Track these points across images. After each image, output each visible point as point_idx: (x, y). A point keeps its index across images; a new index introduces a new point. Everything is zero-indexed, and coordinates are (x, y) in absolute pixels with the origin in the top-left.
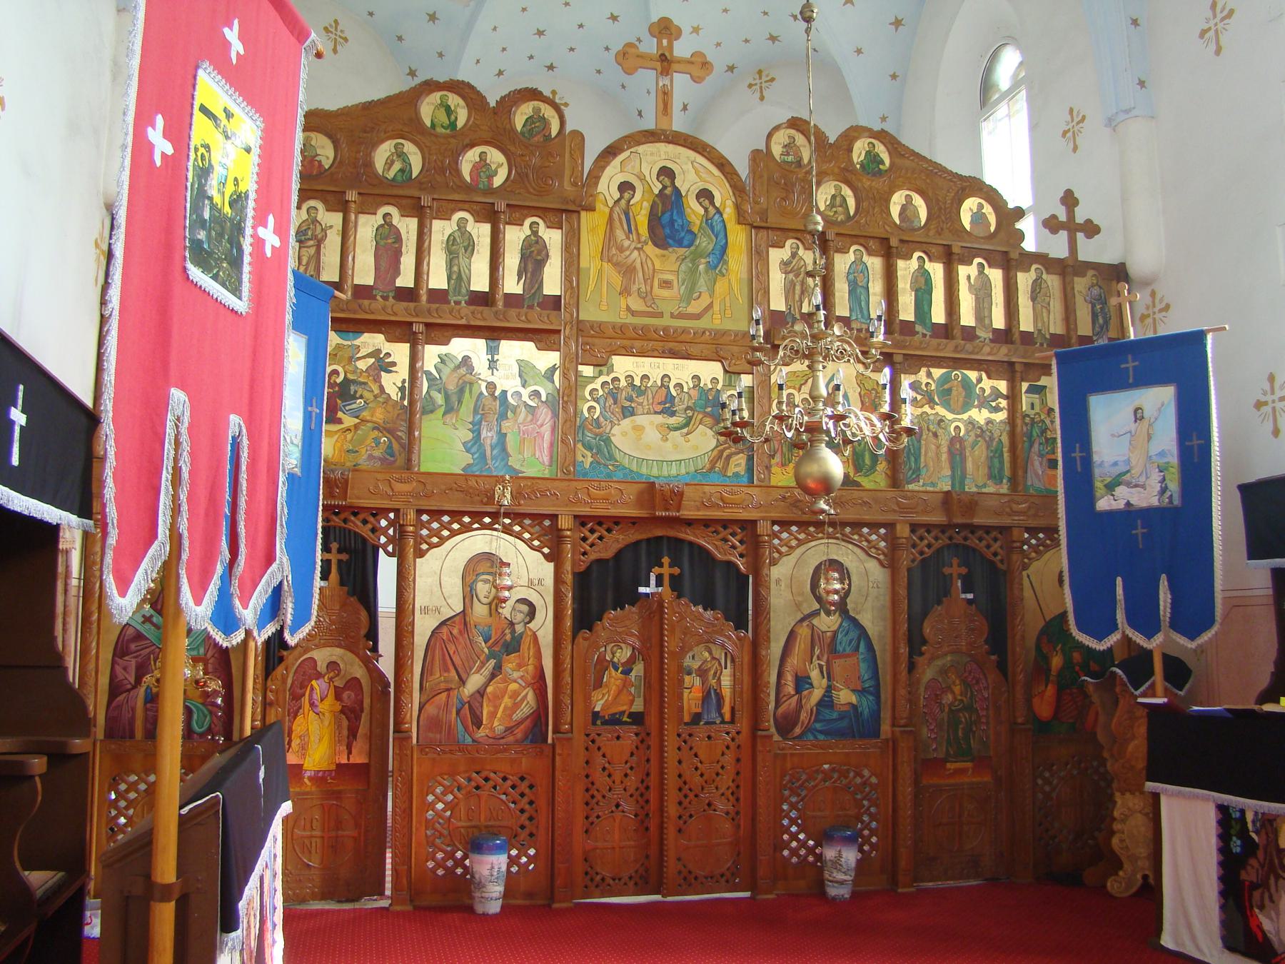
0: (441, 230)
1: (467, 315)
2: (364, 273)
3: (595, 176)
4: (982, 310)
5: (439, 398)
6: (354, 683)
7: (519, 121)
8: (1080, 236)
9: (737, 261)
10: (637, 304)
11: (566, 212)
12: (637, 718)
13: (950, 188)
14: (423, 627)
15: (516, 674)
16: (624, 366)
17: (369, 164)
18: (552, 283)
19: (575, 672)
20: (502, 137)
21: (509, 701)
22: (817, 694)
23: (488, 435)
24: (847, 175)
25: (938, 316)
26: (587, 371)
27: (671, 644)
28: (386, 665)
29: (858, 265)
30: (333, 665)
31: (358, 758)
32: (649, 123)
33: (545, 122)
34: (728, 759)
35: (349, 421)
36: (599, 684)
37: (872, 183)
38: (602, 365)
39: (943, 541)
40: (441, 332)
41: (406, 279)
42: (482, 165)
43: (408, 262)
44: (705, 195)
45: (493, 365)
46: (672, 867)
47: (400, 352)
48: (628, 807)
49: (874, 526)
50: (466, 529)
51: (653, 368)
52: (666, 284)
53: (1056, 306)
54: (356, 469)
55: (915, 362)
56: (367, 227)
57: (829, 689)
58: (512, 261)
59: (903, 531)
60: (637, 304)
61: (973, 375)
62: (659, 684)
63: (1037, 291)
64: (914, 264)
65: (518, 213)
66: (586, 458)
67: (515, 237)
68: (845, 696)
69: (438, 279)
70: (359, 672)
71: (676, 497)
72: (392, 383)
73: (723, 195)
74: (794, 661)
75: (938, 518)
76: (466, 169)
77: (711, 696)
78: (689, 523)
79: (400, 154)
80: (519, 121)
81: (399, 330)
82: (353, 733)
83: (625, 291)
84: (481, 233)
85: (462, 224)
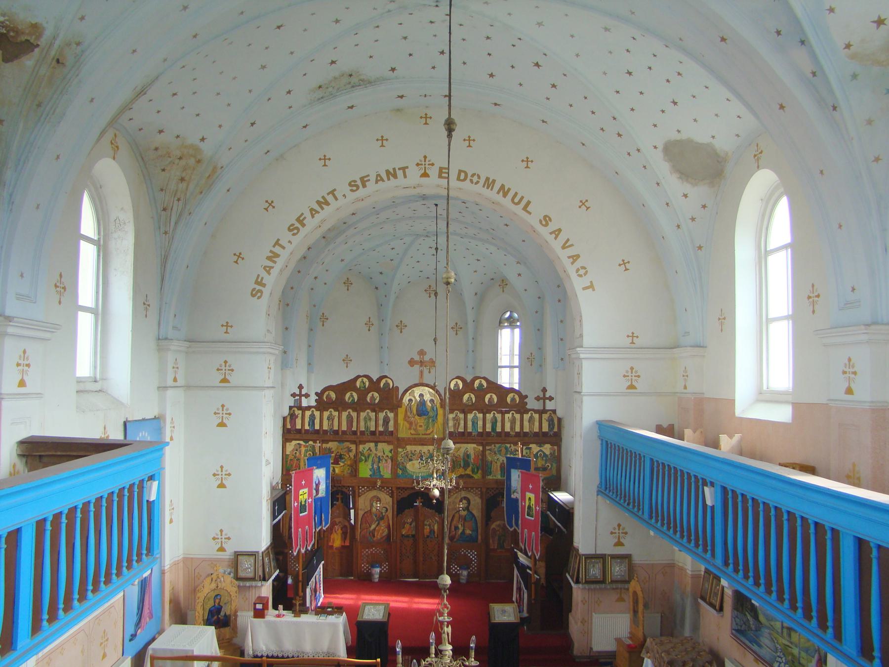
0: (363, 415)
2: (344, 427)
3: (402, 398)
4: (512, 428)
6: (345, 527)
7: (382, 385)
8: (547, 401)
9: (440, 419)
12: (413, 536)
13: (503, 392)
14: (361, 513)
15: (383, 525)
16: (409, 448)
18: (391, 428)
20: (378, 390)
21: (381, 531)
22: (461, 531)
23: (375, 466)
24: (472, 390)
25: (499, 429)
26: (400, 450)
28: (352, 522)
29: (475, 417)
31: (347, 543)
32: (417, 382)
33: (389, 384)
35: (342, 464)
37: (480, 393)
38: (403, 448)
40: (364, 442)
41: (354, 429)
43: (355, 424)
44: (432, 401)
47: (353, 447)
49: (477, 488)
51: (418, 448)
52: (421, 426)
53: (537, 424)
55: (489, 444)
56: (345, 415)
58: (381, 422)
59: (484, 490)
60: (413, 432)
61: (508, 445)
62: (419, 527)
63: (531, 420)
64: (492, 415)
65: (382, 410)
66: (400, 472)
67: (381, 415)
68: (468, 532)
70: (347, 524)
72: (352, 454)
73: (437, 400)
74: (454, 522)
76: (368, 399)
77: (432, 531)
79: (352, 396)
80: (382, 385)
83: (410, 429)
84: (373, 415)
85: (368, 414)
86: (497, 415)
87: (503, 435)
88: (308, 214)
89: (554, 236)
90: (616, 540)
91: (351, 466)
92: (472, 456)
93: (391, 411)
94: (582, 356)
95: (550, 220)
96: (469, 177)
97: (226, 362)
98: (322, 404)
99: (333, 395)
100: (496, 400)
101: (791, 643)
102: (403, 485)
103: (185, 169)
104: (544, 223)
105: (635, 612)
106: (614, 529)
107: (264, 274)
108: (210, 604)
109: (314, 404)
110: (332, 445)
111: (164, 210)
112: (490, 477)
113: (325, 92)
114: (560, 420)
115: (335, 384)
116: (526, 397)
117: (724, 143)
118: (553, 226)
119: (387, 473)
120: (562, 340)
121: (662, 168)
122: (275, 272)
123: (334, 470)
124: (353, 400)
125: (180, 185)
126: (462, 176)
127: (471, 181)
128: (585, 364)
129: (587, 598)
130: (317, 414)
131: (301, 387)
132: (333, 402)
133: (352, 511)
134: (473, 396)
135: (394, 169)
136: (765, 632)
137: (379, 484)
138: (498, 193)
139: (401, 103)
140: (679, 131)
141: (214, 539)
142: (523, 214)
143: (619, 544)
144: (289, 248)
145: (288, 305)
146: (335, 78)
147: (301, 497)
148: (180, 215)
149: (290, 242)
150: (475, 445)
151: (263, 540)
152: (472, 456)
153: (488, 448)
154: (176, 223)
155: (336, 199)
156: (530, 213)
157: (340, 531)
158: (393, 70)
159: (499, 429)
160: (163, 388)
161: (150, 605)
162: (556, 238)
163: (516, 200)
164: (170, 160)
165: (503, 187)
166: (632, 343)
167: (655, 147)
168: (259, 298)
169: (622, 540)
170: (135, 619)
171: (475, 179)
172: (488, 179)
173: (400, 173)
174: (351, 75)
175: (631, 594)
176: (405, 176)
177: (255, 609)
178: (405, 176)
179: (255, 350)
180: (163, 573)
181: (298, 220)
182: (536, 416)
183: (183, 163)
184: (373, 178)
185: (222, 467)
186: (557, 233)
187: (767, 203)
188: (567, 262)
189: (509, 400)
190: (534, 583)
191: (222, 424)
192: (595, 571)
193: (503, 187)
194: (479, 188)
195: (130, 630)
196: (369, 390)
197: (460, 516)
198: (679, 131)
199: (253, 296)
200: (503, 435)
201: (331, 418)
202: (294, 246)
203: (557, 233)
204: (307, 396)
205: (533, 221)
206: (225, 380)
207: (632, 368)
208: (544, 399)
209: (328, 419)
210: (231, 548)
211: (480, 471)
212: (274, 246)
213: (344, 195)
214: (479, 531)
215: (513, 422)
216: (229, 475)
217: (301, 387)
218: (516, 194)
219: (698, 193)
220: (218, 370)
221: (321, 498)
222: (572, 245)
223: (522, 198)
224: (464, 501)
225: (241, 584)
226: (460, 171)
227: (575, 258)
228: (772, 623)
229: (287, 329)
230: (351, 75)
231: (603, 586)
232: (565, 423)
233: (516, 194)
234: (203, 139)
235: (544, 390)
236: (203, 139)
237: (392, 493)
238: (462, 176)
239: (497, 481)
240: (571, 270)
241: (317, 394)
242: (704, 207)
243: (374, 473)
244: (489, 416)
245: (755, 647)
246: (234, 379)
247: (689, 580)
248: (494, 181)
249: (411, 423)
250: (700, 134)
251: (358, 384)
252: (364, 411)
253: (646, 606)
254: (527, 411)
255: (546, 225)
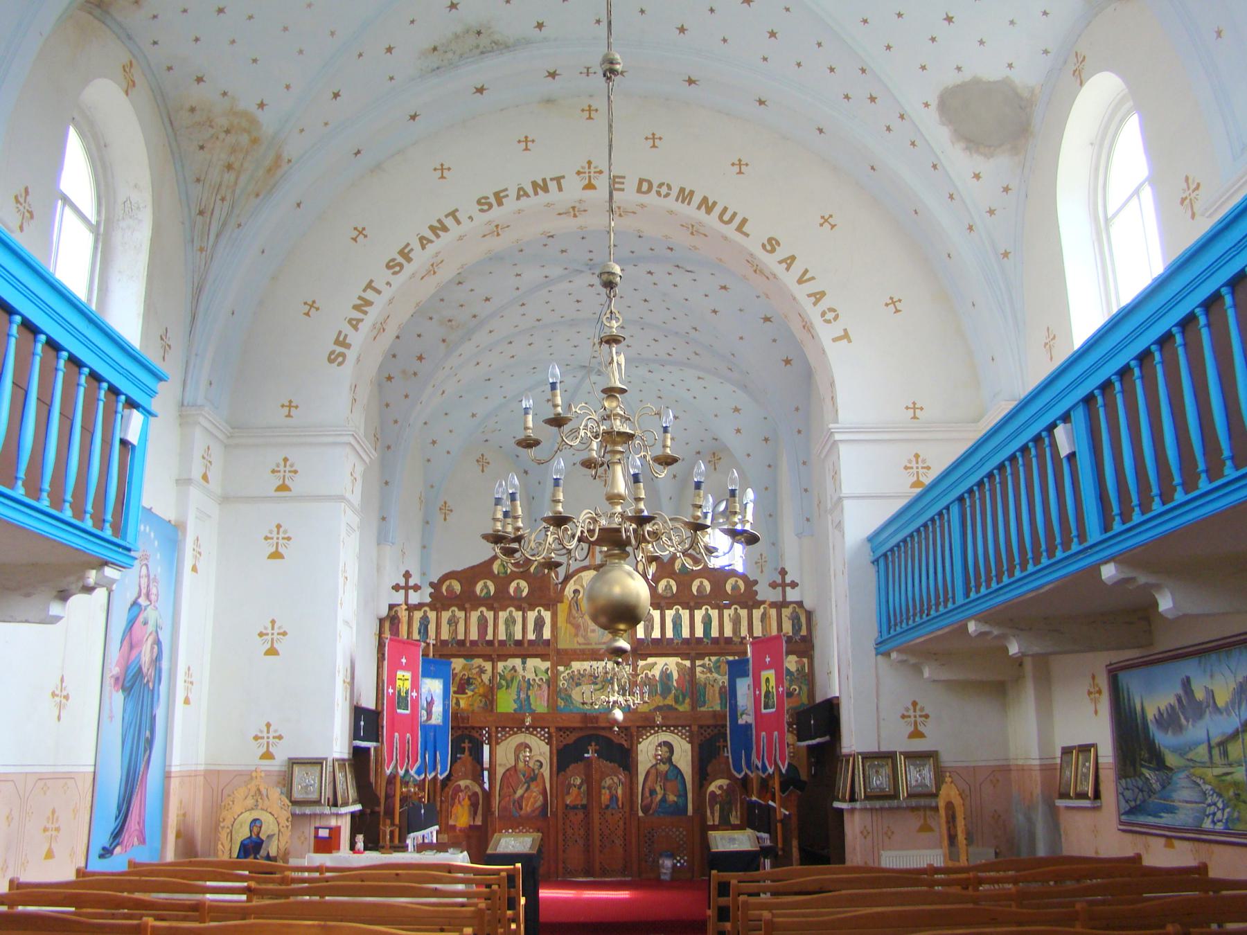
0: (503, 615)
1: (512, 649)
2: (474, 636)
3: (563, 589)
4: (736, 630)
5: (504, 683)
6: (476, 794)
8: (788, 589)
10: (581, 640)
11: (551, 605)
12: (584, 807)
13: (719, 577)
14: (500, 771)
15: (535, 790)
16: (576, 666)
17: (474, 592)
18: (547, 634)
19: (561, 787)
21: (532, 801)
22: (659, 797)
25: (715, 633)
26: (561, 668)
27: (596, 776)
28: (486, 786)
30: (467, 787)
31: (479, 822)
34: (621, 823)
35: (470, 693)
36: (568, 793)
38: (567, 665)
39: (716, 731)
40: (503, 657)
41: (489, 637)
42: (518, 588)
45: (524, 669)
46: (597, 866)
47: (488, 666)
48: (581, 842)
49: (684, 727)
50: (515, 733)
54: (473, 712)
55: (701, 656)
56: (474, 616)
57: (664, 795)
59: (695, 728)
60: (581, 640)
63: (764, 617)
64: (703, 611)
66: (561, 703)
67: (532, 616)
68: (672, 798)
69: (502, 636)
70: (477, 789)
71: (596, 718)
74: (649, 783)
75: (711, 722)
76: (511, 591)
77: (613, 798)
78: (603, 728)
79: (486, 586)
81: (487, 658)
82: (475, 813)
83: (576, 635)
84: (518, 615)
85: (511, 613)
86: (710, 611)
87: (722, 642)
88: (415, 244)
89: (784, 265)
90: (912, 729)
91: (485, 696)
92: (675, 676)
93: (547, 608)
94: (837, 437)
95: (778, 243)
96: (655, 188)
97: (286, 460)
98: (440, 601)
99: (457, 587)
100: (708, 589)
101: (1230, 765)
102: (566, 724)
103: (233, 151)
104: (769, 248)
105: (952, 839)
106: (907, 709)
107: (347, 329)
108: (243, 833)
109: (428, 600)
110: (458, 664)
111: (201, 213)
112: (703, 709)
113: (441, 57)
114: (809, 614)
115: (459, 569)
116: (756, 582)
117: (1026, 76)
118: (781, 253)
119: (540, 706)
120: (806, 490)
121: (939, 135)
122: (365, 327)
123: (458, 703)
124: (489, 592)
125: (226, 176)
126: (645, 186)
127: (659, 193)
128: (843, 448)
129: (870, 829)
130: (432, 615)
131: (407, 575)
132: (457, 597)
133: (486, 773)
134: (673, 583)
135: (544, 180)
136: (1180, 779)
137: (528, 721)
138: (699, 208)
139: (554, 86)
140: (959, 69)
141: (256, 738)
142: (738, 237)
143: (916, 734)
144: (387, 293)
145: (389, 447)
146: (457, 36)
147: (399, 683)
148: (224, 224)
149: (388, 284)
150: (678, 659)
151: (338, 745)
152: (675, 676)
153: (698, 663)
154: (218, 235)
155: (458, 222)
156: (747, 235)
157: (466, 802)
158: (540, 26)
159: (715, 633)
160: (183, 482)
161: (141, 822)
162: (788, 269)
163: (726, 218)
164: (212, 131)
165: (705, 200)
166: (915, 417)
167: (926, 105)
168: (340, 364)
169: (921, 728)
170: (112, 825)
171: (664, 190)
172: (682, 190)
173: (552, 186)
174: (479, 33)
175: (942, 812)
176: (560, 189)
177: (316, 837)
178: (560, 189)
179: (331, 439)
180: (167, 776)
181: (401, 253)
182: (773, 612)
183: (231, 139)
184: (513, 193)
185: (273, 622)
186: (790, 261)
187: (1101, 146)
188: (807, 304)
189: (728, 588)
190: (781, 821)
191: (276, 555)
192: (880, 780)
193: (705, 200)
194: (671, 203)
195: (103, 839)
196: (513, 576)
197: (658, 773)
198: (959, 69)
199: (331, 361)
200: (722, 642)
201: (453, 622)
202: (398, 297)
203: (790, 261)
204: (416, 588)
205: (753, 245)
206: (283, 488)
207: (917, 456)
208: (784, 585)
209: (450, 622)
210: (282, 754)
211: (687, 700)
212: (364, 290)
213: (471, 218)
214: (690, 796)
215: (736, 622)
216: (284, 634)
217: (407, 575)
218: (725, 209)
219: (996, 167)
220: (273, 471)
221: (435, 726)
222: (813, 278)
223: (735, 214)
224: (665, 749)
225: (298, 810)
226: (641, 181)
227: (818, 296)
228: (1190, 756)
229: (387, 483)
230: (479, 33)
231: (895, 803)
232: (818, 618)
233: (725, 209)
234: (262, 105)
235: (783, 572)
236: (262, 105)
237: (550, 738)
238: (645, 186)
239: (715, 715)
240: (813, 314)
241: (432, 585)
242: (1006, 189)
243: (521, 707)
244: (699, 614)
245: (1166, 819)
246: (297, 485)
247: (1037, 776)
248: (692, 193)
249: (577, 627)
250: (989, 68)
251: (496, 567)
252: (505, 610)
253: (970, 839)
254: (758, 604)
255: (773, 251)
